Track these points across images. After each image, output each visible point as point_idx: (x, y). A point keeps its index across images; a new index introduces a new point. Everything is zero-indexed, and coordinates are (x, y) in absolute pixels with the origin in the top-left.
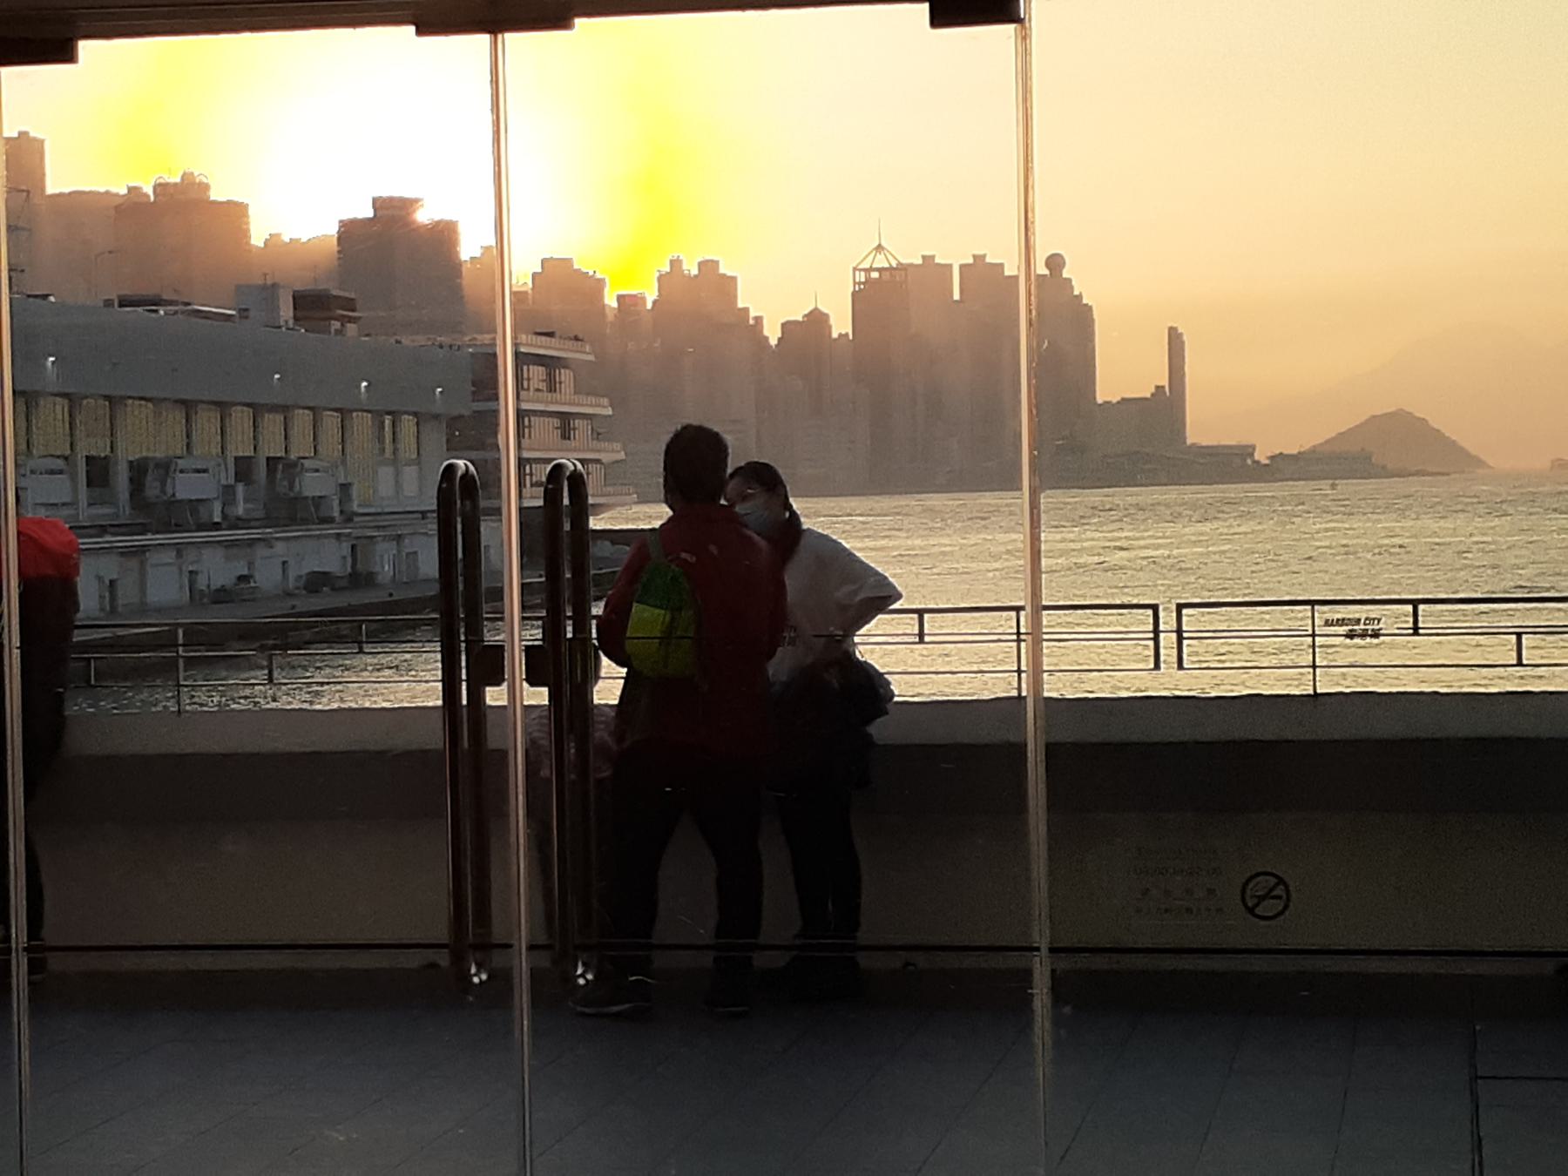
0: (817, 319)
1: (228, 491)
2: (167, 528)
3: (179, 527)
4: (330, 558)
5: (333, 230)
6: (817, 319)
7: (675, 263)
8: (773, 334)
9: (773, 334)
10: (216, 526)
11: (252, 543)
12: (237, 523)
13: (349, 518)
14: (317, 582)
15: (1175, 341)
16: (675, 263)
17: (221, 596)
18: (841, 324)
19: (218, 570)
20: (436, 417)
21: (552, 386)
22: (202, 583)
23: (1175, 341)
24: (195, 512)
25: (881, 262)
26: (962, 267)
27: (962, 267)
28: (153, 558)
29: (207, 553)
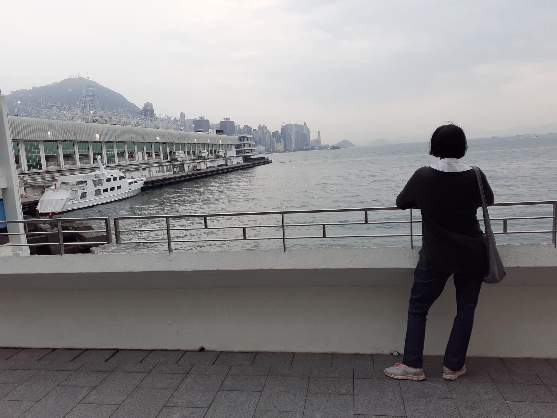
0: (277, 132)
1: (208, 155)
2: (201, 159)
3: (203, 159)
4: (222, 162)
5: (219, 123)
6: (277, 132)
7: (260, 125)
8: (272, 133)
9: (272, 133)
10: (206, 159)
11: (213, 161)
12: (209, 159)
13: (225, 157)
14: (222, 165)
15: (319, 132)
16: (260, 125)
17: (210, 167)
18: (280, 132)
19: (210, 164)
20: (234, 145)
21: (248, 140)
22: (207, 166)
23: (319, 132)
24: (204, 157)
25: (284, 124)
26: (294, 124)
27: (294, 124)
28: (201, 163)
29: (208, 162)
